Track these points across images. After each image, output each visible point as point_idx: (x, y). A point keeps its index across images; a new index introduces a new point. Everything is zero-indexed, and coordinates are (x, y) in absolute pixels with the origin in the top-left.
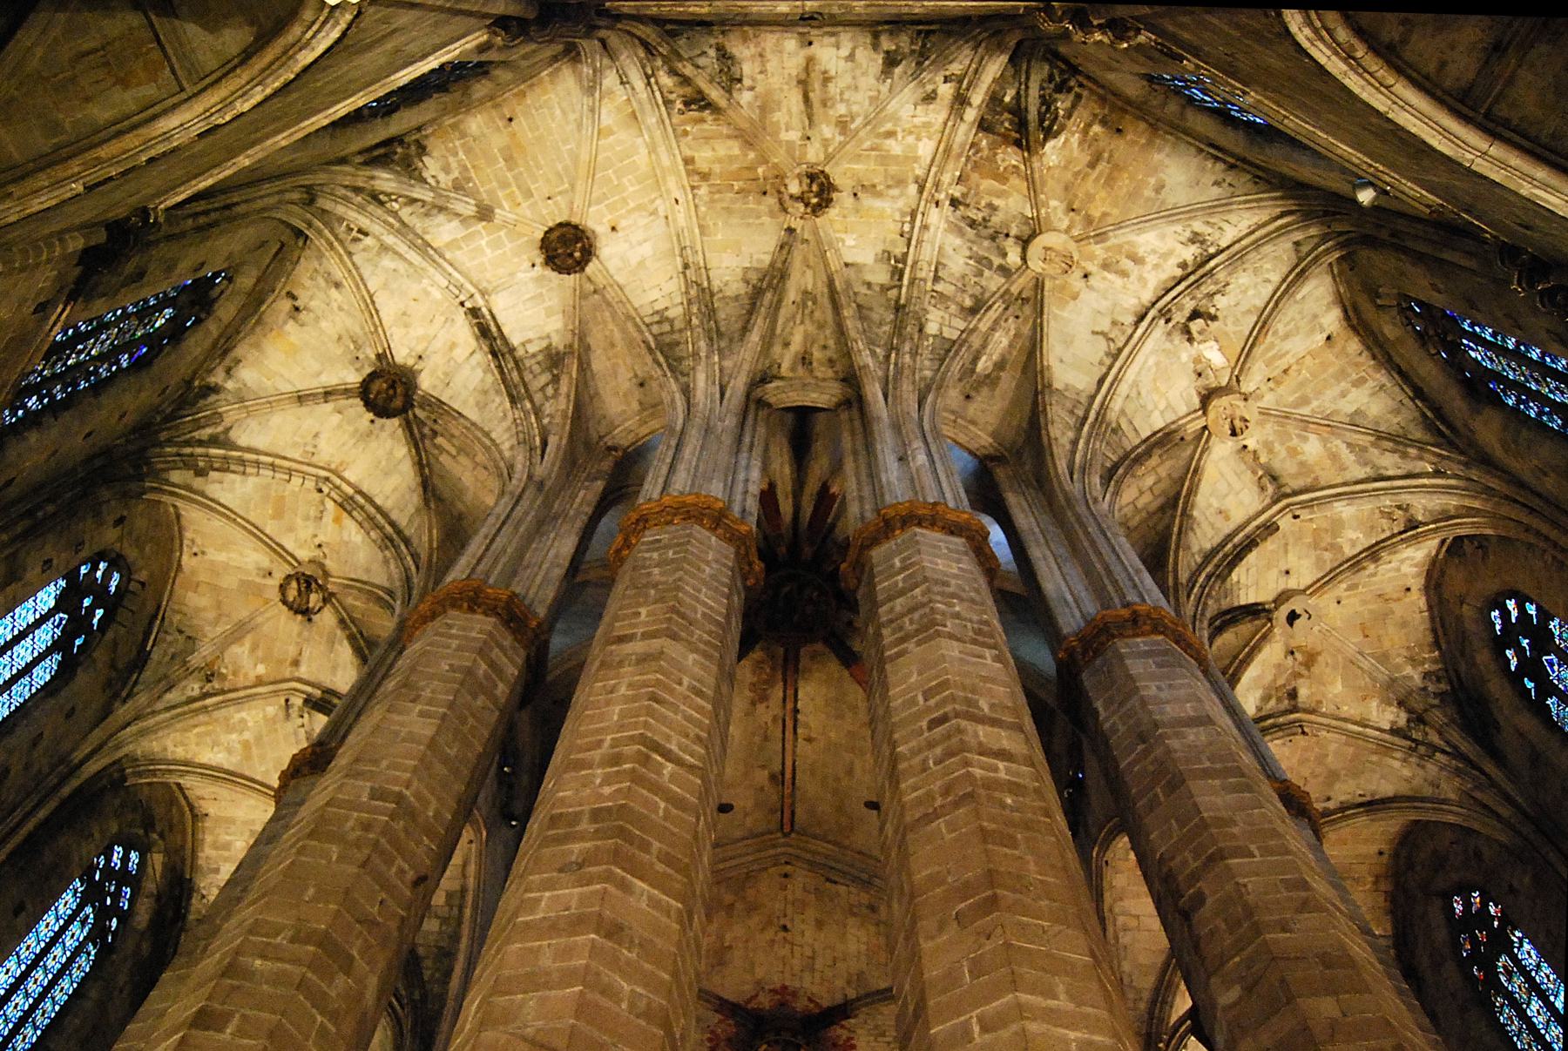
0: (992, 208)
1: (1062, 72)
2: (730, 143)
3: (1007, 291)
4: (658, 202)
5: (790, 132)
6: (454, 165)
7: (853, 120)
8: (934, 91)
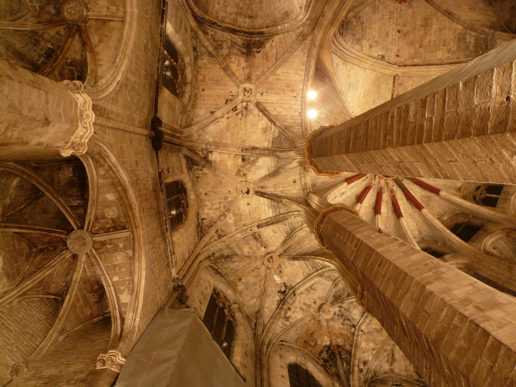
0: (342, 324)
1: (326, 366)
8: (364, 366)
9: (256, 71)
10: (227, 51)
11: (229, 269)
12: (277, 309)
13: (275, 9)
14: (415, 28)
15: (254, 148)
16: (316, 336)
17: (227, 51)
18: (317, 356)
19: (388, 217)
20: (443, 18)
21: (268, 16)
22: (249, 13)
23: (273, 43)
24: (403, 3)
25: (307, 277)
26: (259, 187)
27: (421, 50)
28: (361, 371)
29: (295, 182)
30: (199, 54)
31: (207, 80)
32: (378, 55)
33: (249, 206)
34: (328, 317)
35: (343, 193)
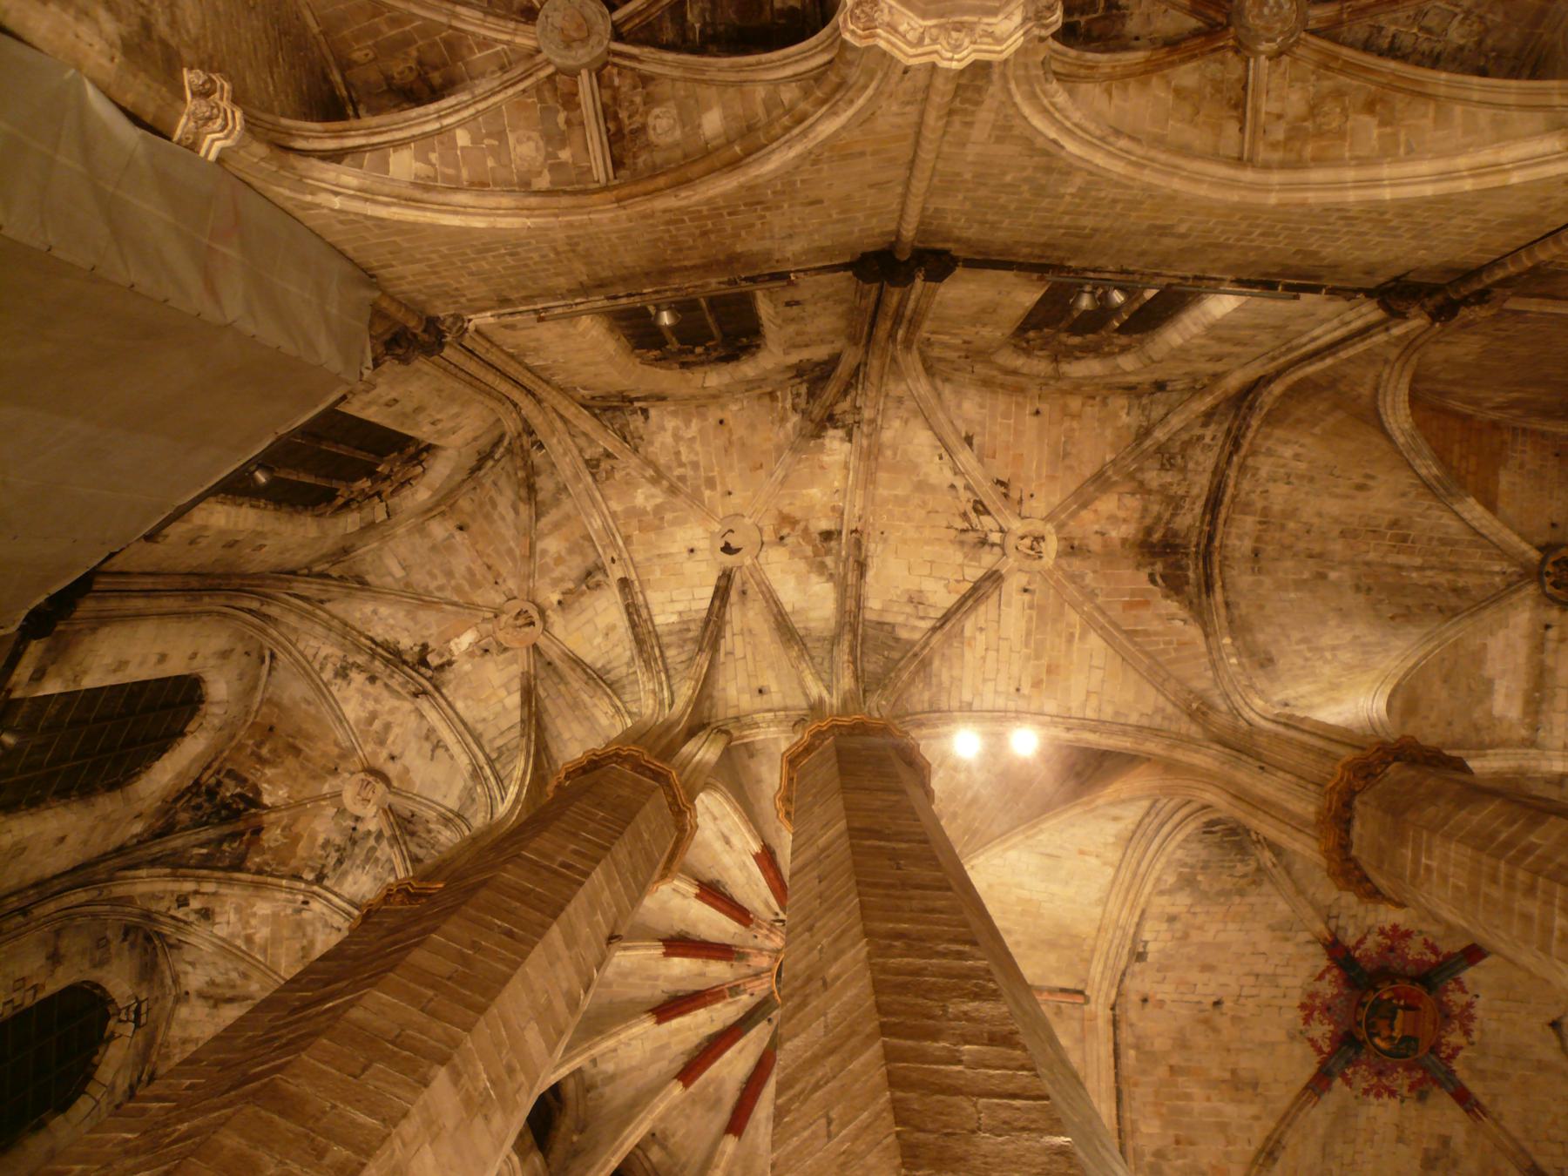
0: (327, 843)
1: (197, 794)
8: (197, 912)
9: (1095, 572)
10: (1155, 485)
11: (493, 493)
12: (372, 640)
13: (1282, 626)
14: (1229, 1050)
15: (862, 567)
16: (291, 762)
17: (1155, 485)
18: (229, 766)
19: (656, 978)
20: (1259, 1134)
21: (1261, 607)
22: (1270, 550)
23: (1179, 623)
24: (1302, 1014)
25: (470, 733)
26: (744, 583)
27: (1162, 1071)
28: (183, 901)
29: (760, 691)
30: (1145, 401)
31: (1067, 424)
32: (1146, 942)
33: (686, 554)
34: (349, 798)
35: (727, 842)
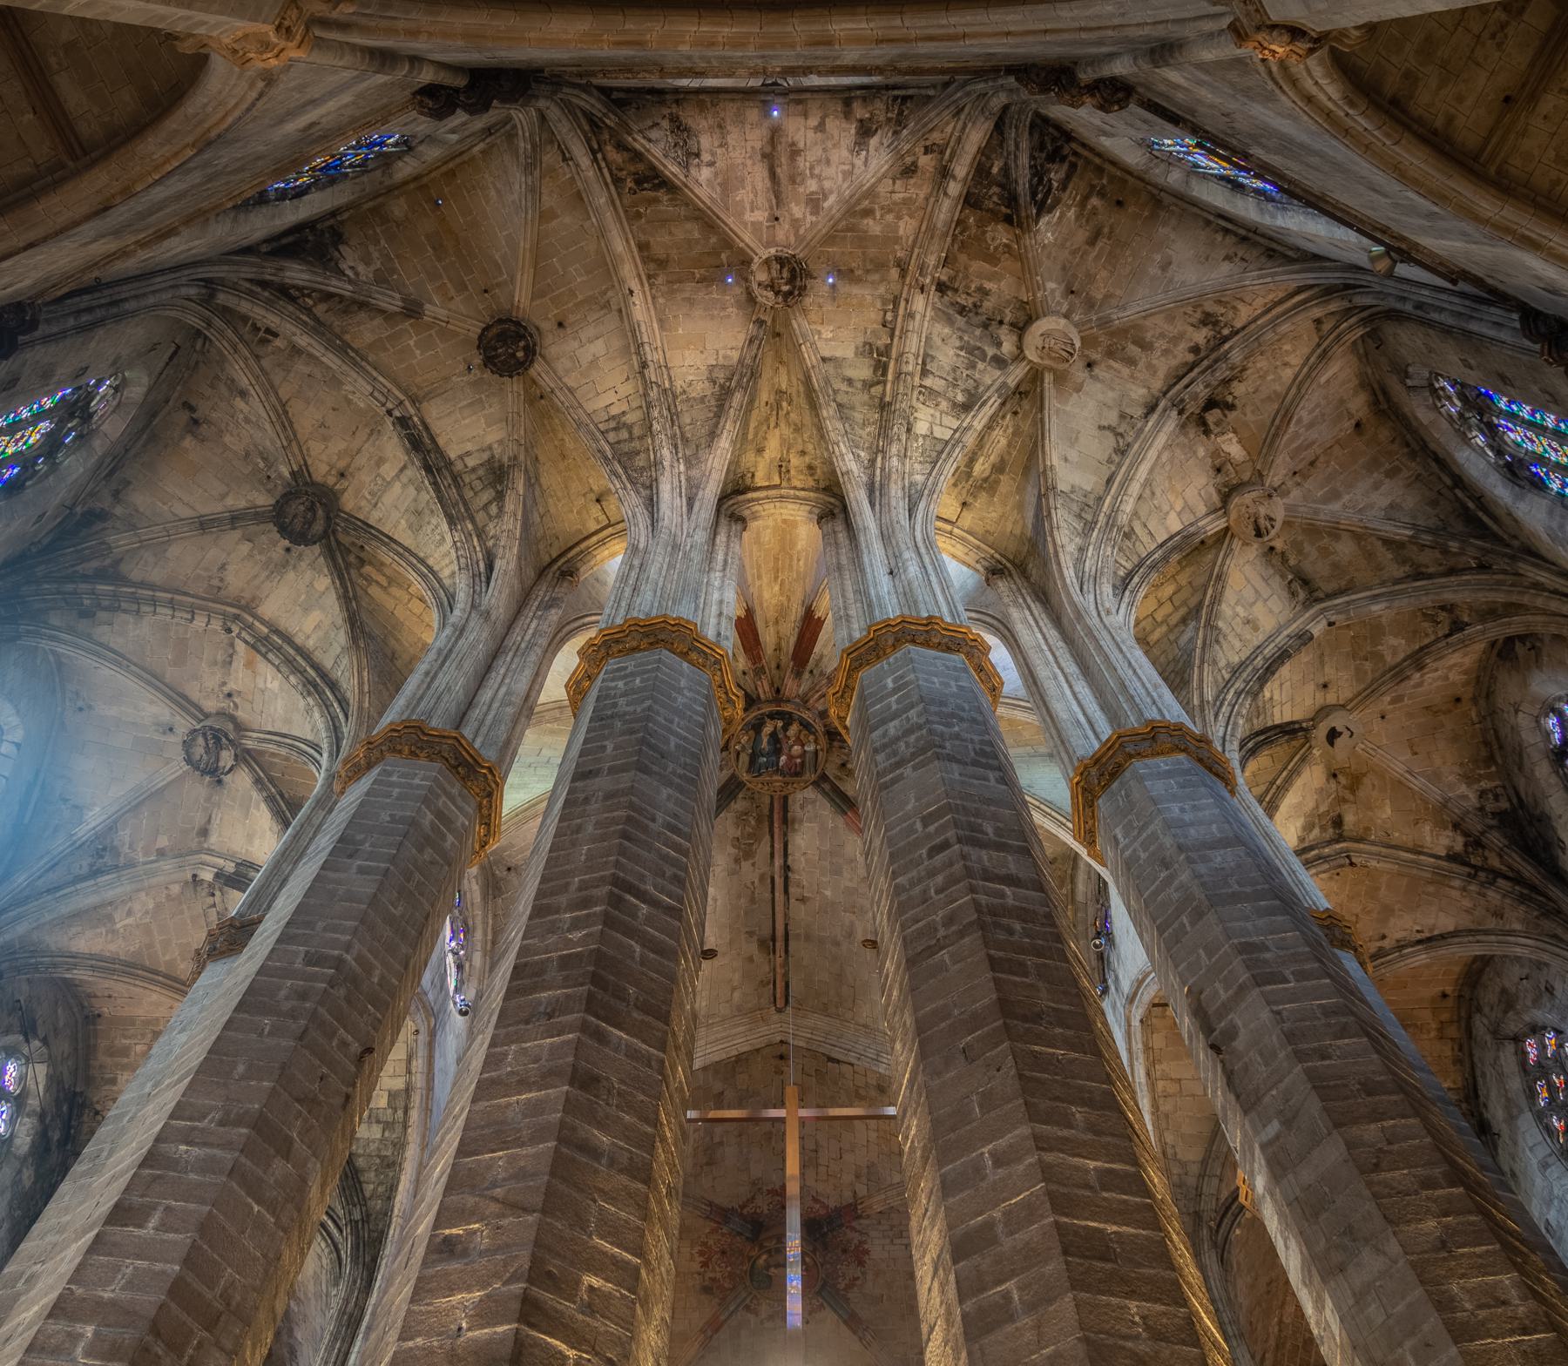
0: (985, 293)
1: (1054, 139)
2: (688, 226)
3: (1004, 384)
4: (610, 294)
5: (756, 213)
6: (375, 255)
7: (825, 198)
8: (914, 164)
11: (1405, 473)
16: (1082, 236)
18: (1080, 163)
33: (1322, 681)
